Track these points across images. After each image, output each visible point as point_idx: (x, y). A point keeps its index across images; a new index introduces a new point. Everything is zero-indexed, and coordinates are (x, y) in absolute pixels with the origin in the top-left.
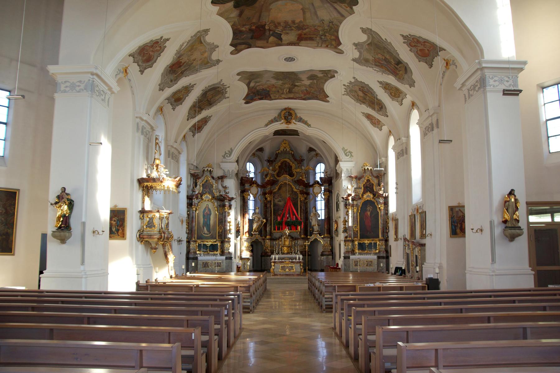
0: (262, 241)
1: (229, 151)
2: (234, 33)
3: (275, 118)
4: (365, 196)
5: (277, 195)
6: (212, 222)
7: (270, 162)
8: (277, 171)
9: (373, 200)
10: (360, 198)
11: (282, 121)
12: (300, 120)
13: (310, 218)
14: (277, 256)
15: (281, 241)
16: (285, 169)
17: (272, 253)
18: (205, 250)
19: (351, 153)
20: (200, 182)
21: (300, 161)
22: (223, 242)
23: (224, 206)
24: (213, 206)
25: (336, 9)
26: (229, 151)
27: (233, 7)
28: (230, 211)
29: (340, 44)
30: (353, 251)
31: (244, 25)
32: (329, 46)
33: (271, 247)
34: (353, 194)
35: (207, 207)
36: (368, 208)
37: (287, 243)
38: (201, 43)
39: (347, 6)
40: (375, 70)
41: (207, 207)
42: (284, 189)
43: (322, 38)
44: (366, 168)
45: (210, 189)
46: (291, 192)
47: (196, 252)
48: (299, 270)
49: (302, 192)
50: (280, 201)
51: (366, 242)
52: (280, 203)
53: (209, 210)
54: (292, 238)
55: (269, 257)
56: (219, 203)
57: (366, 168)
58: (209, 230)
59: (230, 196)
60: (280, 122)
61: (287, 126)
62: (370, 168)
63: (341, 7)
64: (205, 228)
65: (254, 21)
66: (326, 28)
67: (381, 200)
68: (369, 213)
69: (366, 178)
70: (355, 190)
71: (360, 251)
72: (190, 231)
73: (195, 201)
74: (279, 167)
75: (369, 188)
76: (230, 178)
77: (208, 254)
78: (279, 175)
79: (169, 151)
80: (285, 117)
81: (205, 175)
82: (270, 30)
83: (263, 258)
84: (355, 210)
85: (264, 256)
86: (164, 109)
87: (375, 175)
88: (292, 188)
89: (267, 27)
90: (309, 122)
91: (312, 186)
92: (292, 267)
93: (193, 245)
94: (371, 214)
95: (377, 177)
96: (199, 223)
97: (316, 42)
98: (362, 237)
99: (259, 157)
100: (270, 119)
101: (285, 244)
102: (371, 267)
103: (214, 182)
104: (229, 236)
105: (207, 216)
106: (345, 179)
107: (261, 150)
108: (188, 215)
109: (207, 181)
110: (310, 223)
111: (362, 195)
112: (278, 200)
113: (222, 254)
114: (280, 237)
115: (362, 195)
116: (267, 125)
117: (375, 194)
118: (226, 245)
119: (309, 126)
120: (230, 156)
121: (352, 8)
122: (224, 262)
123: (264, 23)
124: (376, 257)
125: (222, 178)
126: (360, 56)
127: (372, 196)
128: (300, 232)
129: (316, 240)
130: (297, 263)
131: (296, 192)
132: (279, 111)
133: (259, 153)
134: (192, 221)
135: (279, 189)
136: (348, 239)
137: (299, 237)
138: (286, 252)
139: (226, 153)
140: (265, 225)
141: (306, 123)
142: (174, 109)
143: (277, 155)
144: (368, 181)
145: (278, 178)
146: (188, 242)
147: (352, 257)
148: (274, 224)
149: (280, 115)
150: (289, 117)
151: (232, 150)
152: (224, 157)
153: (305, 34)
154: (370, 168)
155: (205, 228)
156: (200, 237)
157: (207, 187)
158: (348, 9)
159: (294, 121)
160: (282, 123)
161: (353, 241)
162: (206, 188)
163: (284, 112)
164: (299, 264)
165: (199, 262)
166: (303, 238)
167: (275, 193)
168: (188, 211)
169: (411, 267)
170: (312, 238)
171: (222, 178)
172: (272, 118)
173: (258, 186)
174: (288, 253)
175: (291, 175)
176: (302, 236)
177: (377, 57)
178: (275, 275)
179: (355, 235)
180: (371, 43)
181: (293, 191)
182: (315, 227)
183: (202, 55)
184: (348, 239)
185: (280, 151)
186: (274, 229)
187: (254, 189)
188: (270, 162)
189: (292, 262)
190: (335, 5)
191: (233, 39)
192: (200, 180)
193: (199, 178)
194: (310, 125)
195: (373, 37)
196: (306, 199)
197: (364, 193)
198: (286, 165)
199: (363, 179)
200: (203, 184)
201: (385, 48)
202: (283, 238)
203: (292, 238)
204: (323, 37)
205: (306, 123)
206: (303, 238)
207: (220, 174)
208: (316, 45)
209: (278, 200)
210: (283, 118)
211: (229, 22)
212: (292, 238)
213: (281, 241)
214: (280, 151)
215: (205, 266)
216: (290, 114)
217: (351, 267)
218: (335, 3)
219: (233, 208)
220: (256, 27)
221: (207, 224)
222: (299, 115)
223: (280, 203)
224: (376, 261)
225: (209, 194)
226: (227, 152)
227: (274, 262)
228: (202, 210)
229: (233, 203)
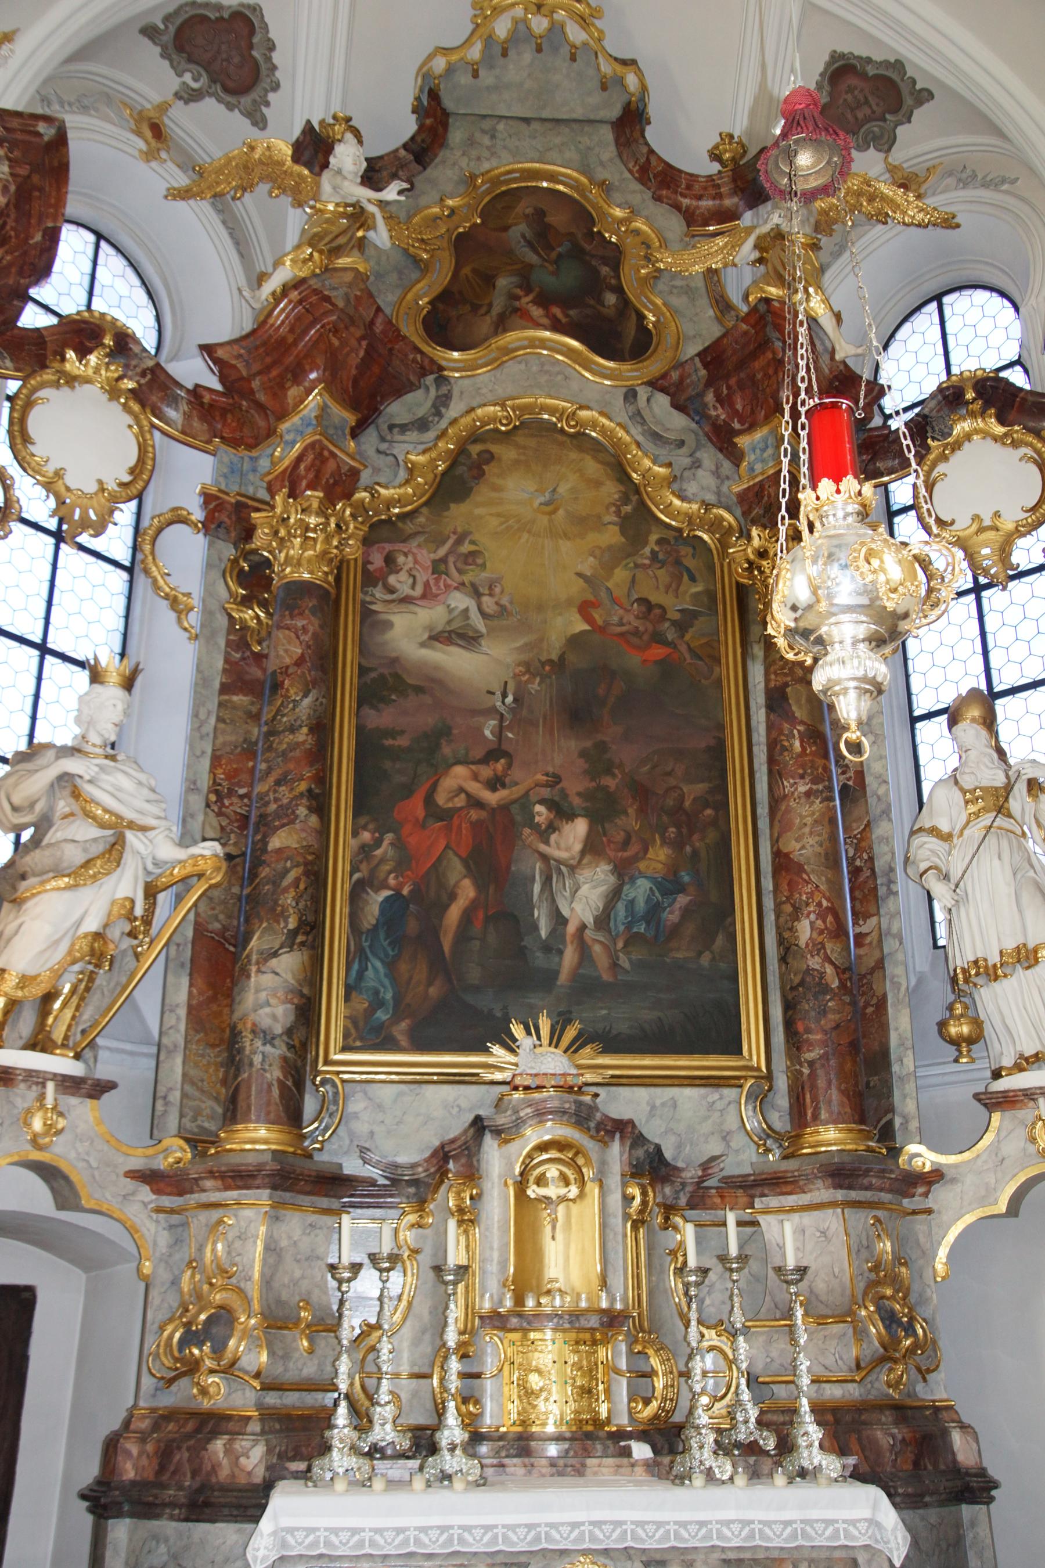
5: (414, 562)
15: (468, 1218)
16: (543, 261)
17: (300, 1439)
33: (278, 1321)
37: (574, 1256)
42: (515, 490)
46: (611, 536)
52: (455, 661)
54: (652, 1167)
55: (222, 1534)
83: (121, 1531)
85: (143, 1502)
88: (631, 491)
101: (526, 1278)
114: (455, 1160)
137: (744, 1159)
138: (553, 1412)
140: (217, 962)
148: (357, 956)
166: (842, 1173)
173: (149, 388)
174: (591, 1441)
175: (615, 333)
176: (830, 1137)
181: (636, 514)
186: (369, 1035)
198: (543, 235)
203: (652, 1167)
206: (842, 1173)
213: (468, 1218)
223: (455, 661)
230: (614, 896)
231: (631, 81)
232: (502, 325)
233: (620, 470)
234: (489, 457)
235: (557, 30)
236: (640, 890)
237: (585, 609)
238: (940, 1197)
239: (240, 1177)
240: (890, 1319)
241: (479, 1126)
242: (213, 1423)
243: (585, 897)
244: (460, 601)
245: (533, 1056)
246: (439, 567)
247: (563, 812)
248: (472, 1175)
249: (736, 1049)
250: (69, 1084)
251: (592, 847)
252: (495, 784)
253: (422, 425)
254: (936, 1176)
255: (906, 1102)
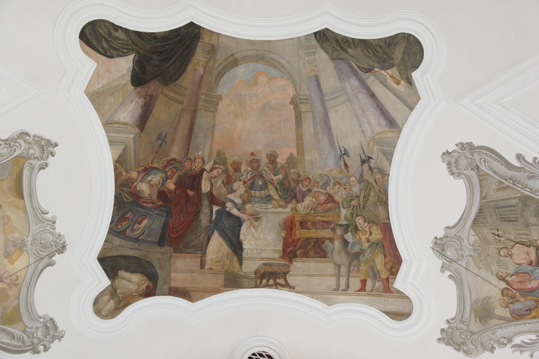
2: (119, 203)
25: (372, 96)
27: (129, 78)
29: (395, 261)
31: (148, 170)
32: (369, 285)
38: (19, 192)
39: (397, 75)
40: (520, 347)
43: (346, 243)
63: (383, 83)
65: (175, 152)
66: (356, 189)
82: (213, 200)
89: (205, 187)
97: (330, 268)
121: (410, 82)
123: (198, 164)
126: (461, 299)
153: (303, 224)
158: (403, 87)
177: (512, 269)
180: (481, 211)
183: (7, 255)
190: (370, 80)
191: (115, 230)
195: (482, 177)
201: (525, 200)
204: (349, 237)
208: (333, 281)
211: (112, 143)
218: (368, 70)
220: (178, 184)
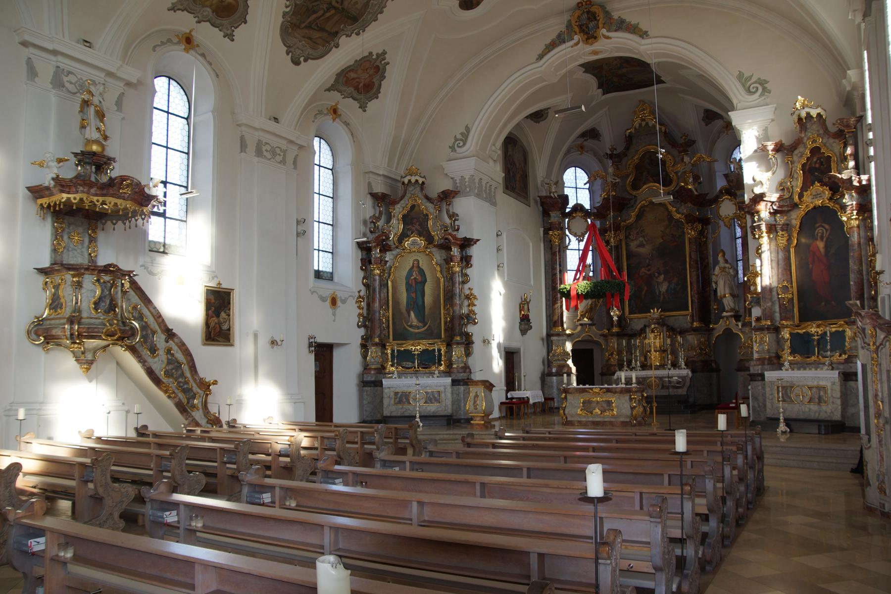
0: (601, 340)
1: (462, 134)
3: (559, 36)
4: (807, 197)
6: (428, 299)
7: (616, 157)
8: (630, 179)
9: (830, 205)
10: (795, 206)
11: (576, 38)
12: (622, 26)
13: (714, 278)
14: (634, 375)
18: (410, 364)
19: (762, 83)
20: (399, 210)
21: (682, 145)
22: (449, 345)
23: (449, 260)
24: (431, 263)
26: (462, 134)
28: (468, 271)
30: (778, 357)
34: (774, 197)
35: (416, 266)
36: (819, 231)
41: (416, 266)
44: (803, 114)
45: (420, 225)
47: (384, 368)
48: (627, 411)
49: (690, 219)
50: (642, 245)
51: (813, 330)
53: (422, 272)
56: (444, 254)
57: (803, 114)
58: (421, 317)
59: (461, 235)
60: (572, 43)
61: (589, 48)
62: (814, 113)
64: (412, 314)
67: (850, 200)
68: (821, 245)
69: (810, 145)
70: (782, 187)
71: (798, 358)
72: (368, 321)
73: (376, 253)
74: (637, 167)
75: (818, 169)
76: (467, 195)
77: (416, 373)
78: (636, 186)
79: (242, 138)
80: (580, 27)
81: (408, 195)
84: (783, 241)
86: (198, 37)
87: (833, 129)
88: (669, 212)
90: (644, 27)
91: (716, 200)
92: (609, 403)
93: (373, 351)
94: (826, 247)
95: (840, 135)
96: (396, 303)
98: (806, 316)
99: (595, 154)
100: (548, 41)
102: (824, 407)
103: (430, 206)
104: (470, 329)
105: (416, 284)
106: (750, 159)
107: (592, 134)
108: (367, 286)
109: (413, 207)
110: (715, 291)
111: (801, 196)
112: (636, 243)
113: (448, 373)
114: (643, 331)
115: (801, 196)
116: (541, 57)
117: (837, 188)
118: (457, 352)
119: (643, 34)
120: (464, 144)
122: (449, 389)
124: (835, 374)
125: (447, 196)
127: (827, 193)
128: (692, 317)
129: (728, 332)
130: (623, 391)
131: (677, 221)
132: (566, 17)
133: (589, 143)
134: (374, 300)
135: (639, 217)
136: (763, 323)
139: (456, 140)
141: (634, 29)
142: (231, 37)
143: (629, 139)
144: (815, 151)
145: (634, 193)
146: (364, 347)
147: (770, 375)
149: (569, 26)
150: (591, 25)
151: (468, 129)
152: (452, 148)
154: (814, 113)
155: (412, 314)
156: (401, 335)
157: (415, 222)
159: (604, 31)
160: (577, 44)
161: (776, 330)
162: (412, 223)
163: (578, 13)
164: (627, 398)
165: (386, 391)
166: (695, 330)
167: (629, 228)
168: (364, 278)
169: (874, 421)
170: (719, 328)
171: (447, 196)
172: (554, 36)
174: (662, 366)
178: (569, 423)
179: (786, 312)
181: (670, 217)
182: (725, 301)
184: (763, 323)
185: (633, 130)
187: (580, 224)
188: (616, 157)
189: (608, 390)
192: (399, 206)
193: (394, 203)
194: (646, 33)
196: (701, 233)
197: (804, 188)
199: (801, 149)
200: (404, 217)
202: (647, 330)
205: (634, 29)
206: (695, 330)
207: (446, 185)
209: (636, 243)
210: (577, 29)
212: (673, 331)
214: (633, 130)
215: (400, 402)
216: (593, 17)
217: (768, 405)
219: (474, 261)
221: (416, 304)
222: (615, 15)
224: (837, 387)
225: (420, 235)
226: (459, 136)
227: (566, 391)
228: (404, 273)
229: (475, 251)
230: (668, 287)
231: (663, 129)
232: (645, 184)
233: (667, 209)
234: (644, 211)
235: (647, 124)
236: (673, 286)
237: (662, 238)
238: (714, 332)
239: (612, 335)
240: (701, 349)
241: (645, 326)
242: (612, 365)
243: (664, 288)
244: (641, 239)
245: (655, 313)
246: (637, 233)
247: (660, 274)
248: (645, 332)
249: (688, 310)
250: (590, 325)
251: (665, 279)
252: (649, 270)
253: (632, 206)
254: (713, 329)
255: (713, 317)
